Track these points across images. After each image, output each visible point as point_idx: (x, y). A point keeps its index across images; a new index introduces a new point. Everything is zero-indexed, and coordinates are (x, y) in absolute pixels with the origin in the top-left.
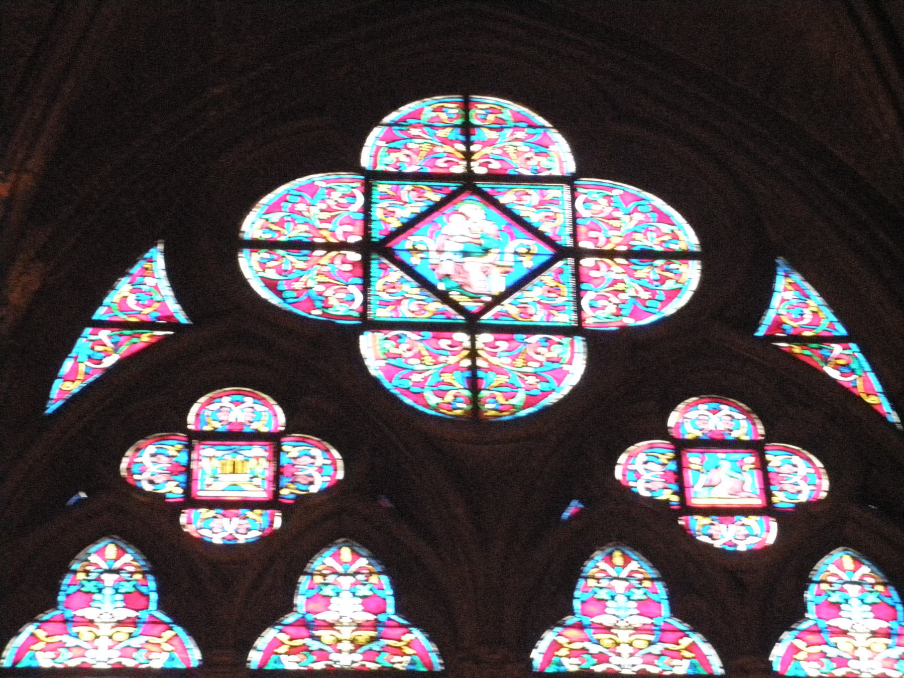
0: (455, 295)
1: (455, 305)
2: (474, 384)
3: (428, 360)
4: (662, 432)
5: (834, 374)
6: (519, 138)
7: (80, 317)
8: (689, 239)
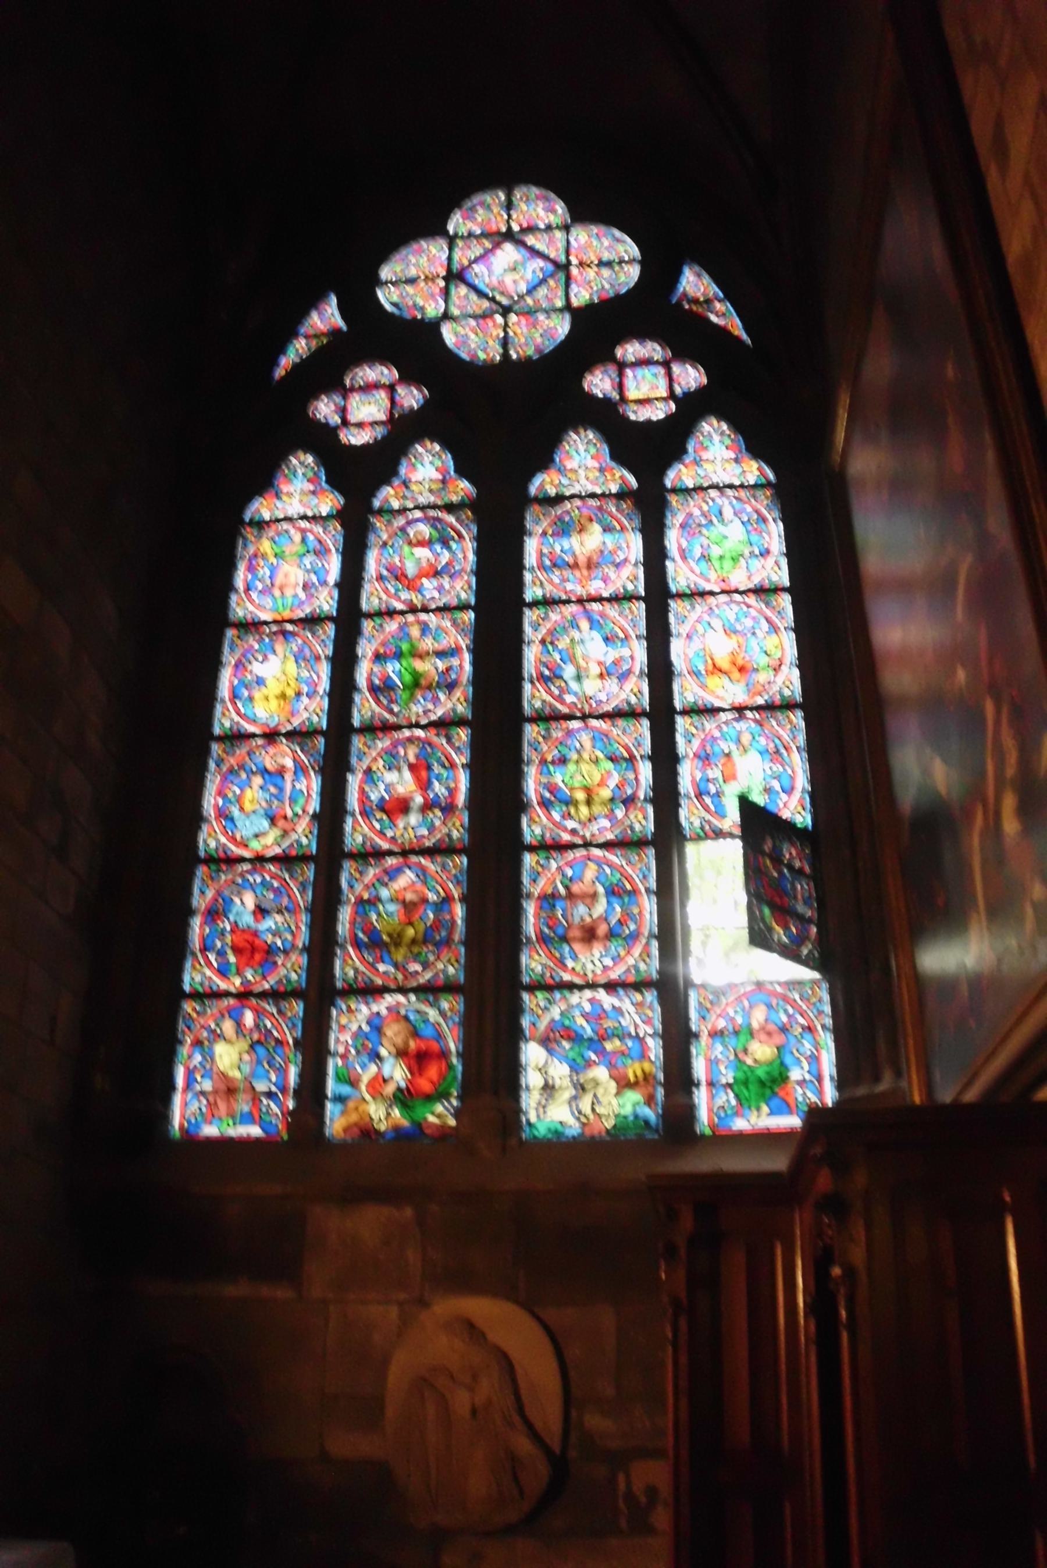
0: (498, 298)
1: (499, 303)
2: (505, 343)
3: (481, 335)
4: (613, 359)
5: (713, 318)
6: (539, 208)
7: (293, 334)
8: (634, 251)
